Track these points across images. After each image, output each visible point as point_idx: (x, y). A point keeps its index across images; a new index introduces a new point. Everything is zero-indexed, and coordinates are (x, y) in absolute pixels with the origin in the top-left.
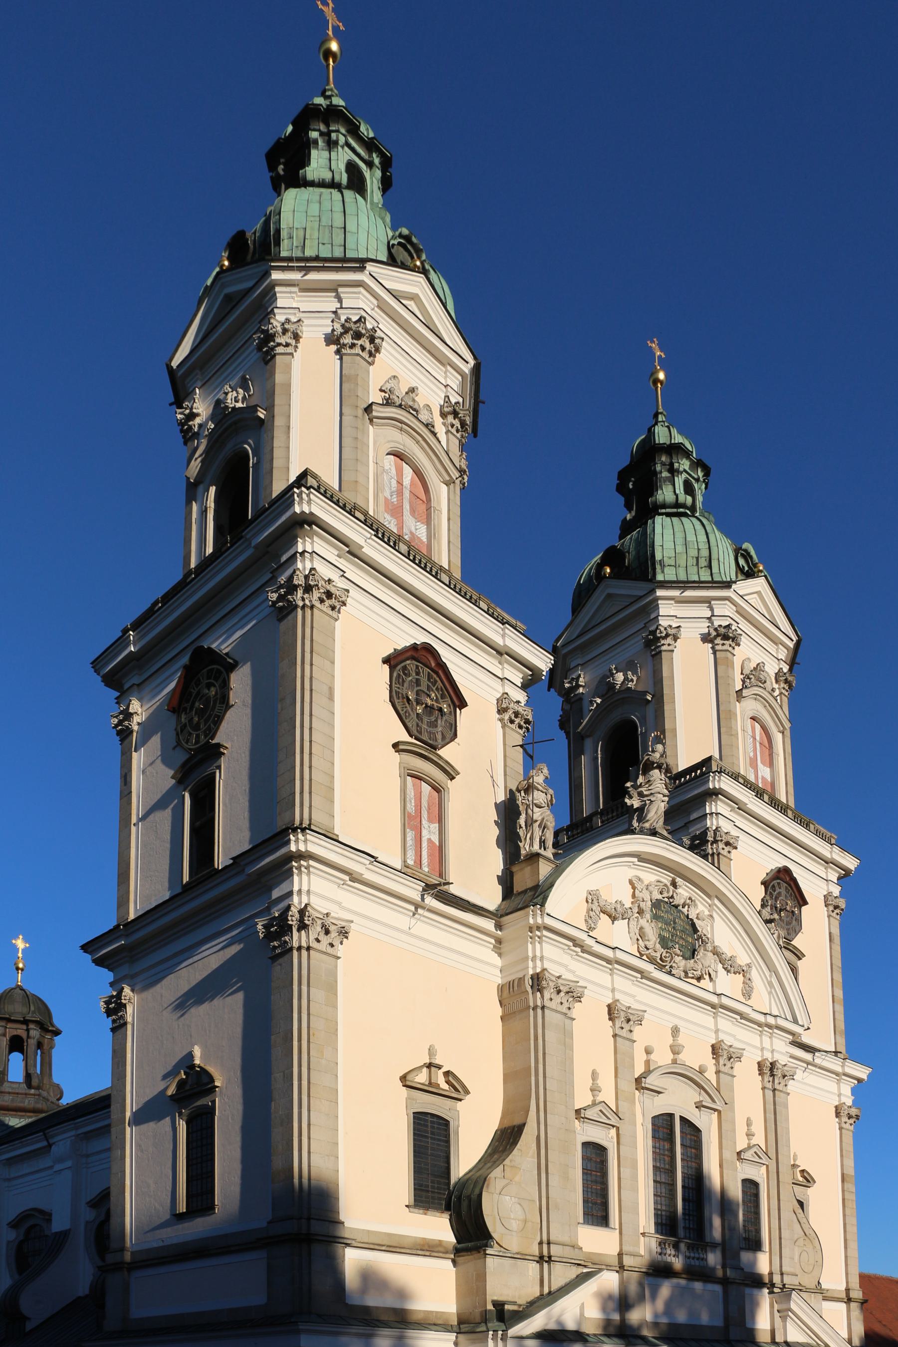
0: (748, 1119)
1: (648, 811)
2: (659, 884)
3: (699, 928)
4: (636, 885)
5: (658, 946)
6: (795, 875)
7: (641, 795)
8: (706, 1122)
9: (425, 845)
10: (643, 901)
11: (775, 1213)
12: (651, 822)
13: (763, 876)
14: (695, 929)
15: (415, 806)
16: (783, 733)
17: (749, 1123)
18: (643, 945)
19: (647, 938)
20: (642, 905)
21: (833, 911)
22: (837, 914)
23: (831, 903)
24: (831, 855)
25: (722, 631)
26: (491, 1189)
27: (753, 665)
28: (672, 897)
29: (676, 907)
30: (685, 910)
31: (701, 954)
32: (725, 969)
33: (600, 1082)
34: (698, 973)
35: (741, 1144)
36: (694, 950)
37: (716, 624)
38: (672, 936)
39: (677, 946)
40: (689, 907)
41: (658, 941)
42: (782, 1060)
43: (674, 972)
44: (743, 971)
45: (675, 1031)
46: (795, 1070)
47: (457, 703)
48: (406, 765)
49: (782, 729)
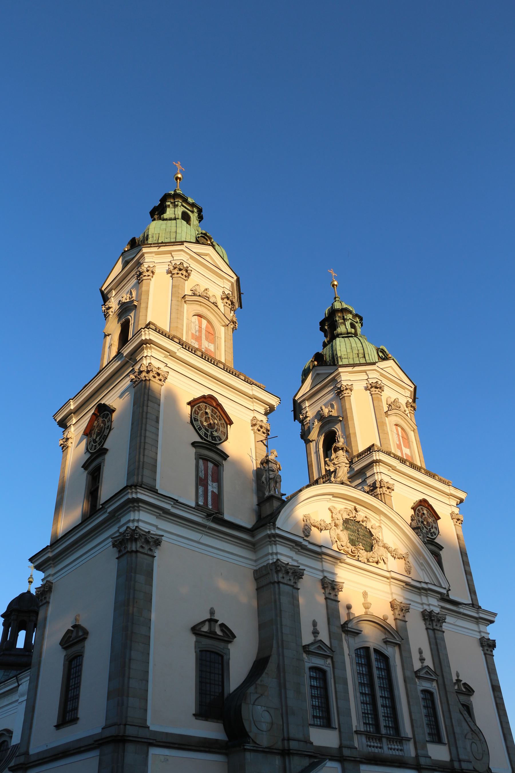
0: (420, 649)
1: (338, 472)
2: (346, 510)
3: (373, 534)
4: (333, 511)
5: (349, 545)
6: (430, 503)
7: (334, 464)
9: (210, 494)
10: (338, 520)
12: (341, 477)
13: (412, 505)
14: (372, 535)
15: (204, 474)
16: (414, 431)
17: (421, 652)
19: (341, 540)
20: (337, 522)
21: (457, 522)
22: (460, 523)
23: (454, 517)
24: (450, 492)
25: (374, 385)
27: (392, 400)
28: (355, 517)
29: (359, 522)
30: (364, 524)
31: (376, 548)
32: (393, 556)
33: (319, 628)
34: (376, 560)
36: (372, 546)
37: (370, 382)
38: (358, 539)
39: (361, 544)
40: (366, 522)
41: (348, 541)
42: (437, 610)
43: (360, 559)
44: (404, 557)
45: (365, 594)
46: (445, 616)
47: (228, 422)
48: (198, 453)
49: (413, 429)
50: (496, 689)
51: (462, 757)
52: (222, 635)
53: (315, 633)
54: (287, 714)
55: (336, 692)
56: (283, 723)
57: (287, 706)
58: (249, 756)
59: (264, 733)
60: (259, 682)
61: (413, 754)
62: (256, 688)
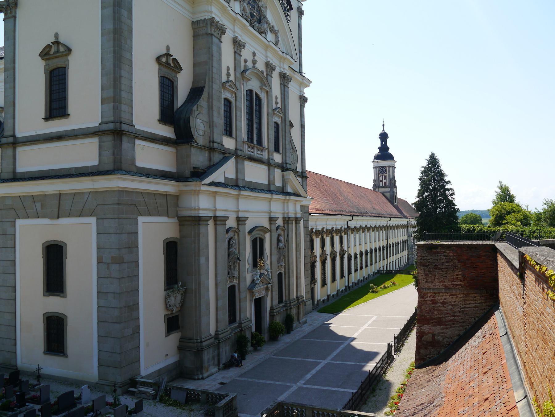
8: (262, 95)
11: (284, 137)
18: (244, 14)
26: (193, 115)
35: (274, 107)
45: (254, 54)
50: (302, 126)
51: (288, 162)
52: (173, 66)
53: (228, 75)
54: (213, 126)
55: (236, 116)
56: (210, 132)
57: (213, 121)
58: (193, 150)
59: (201, 137)
60: (198, 103)
61: (267, 158)
62: (197, 107)
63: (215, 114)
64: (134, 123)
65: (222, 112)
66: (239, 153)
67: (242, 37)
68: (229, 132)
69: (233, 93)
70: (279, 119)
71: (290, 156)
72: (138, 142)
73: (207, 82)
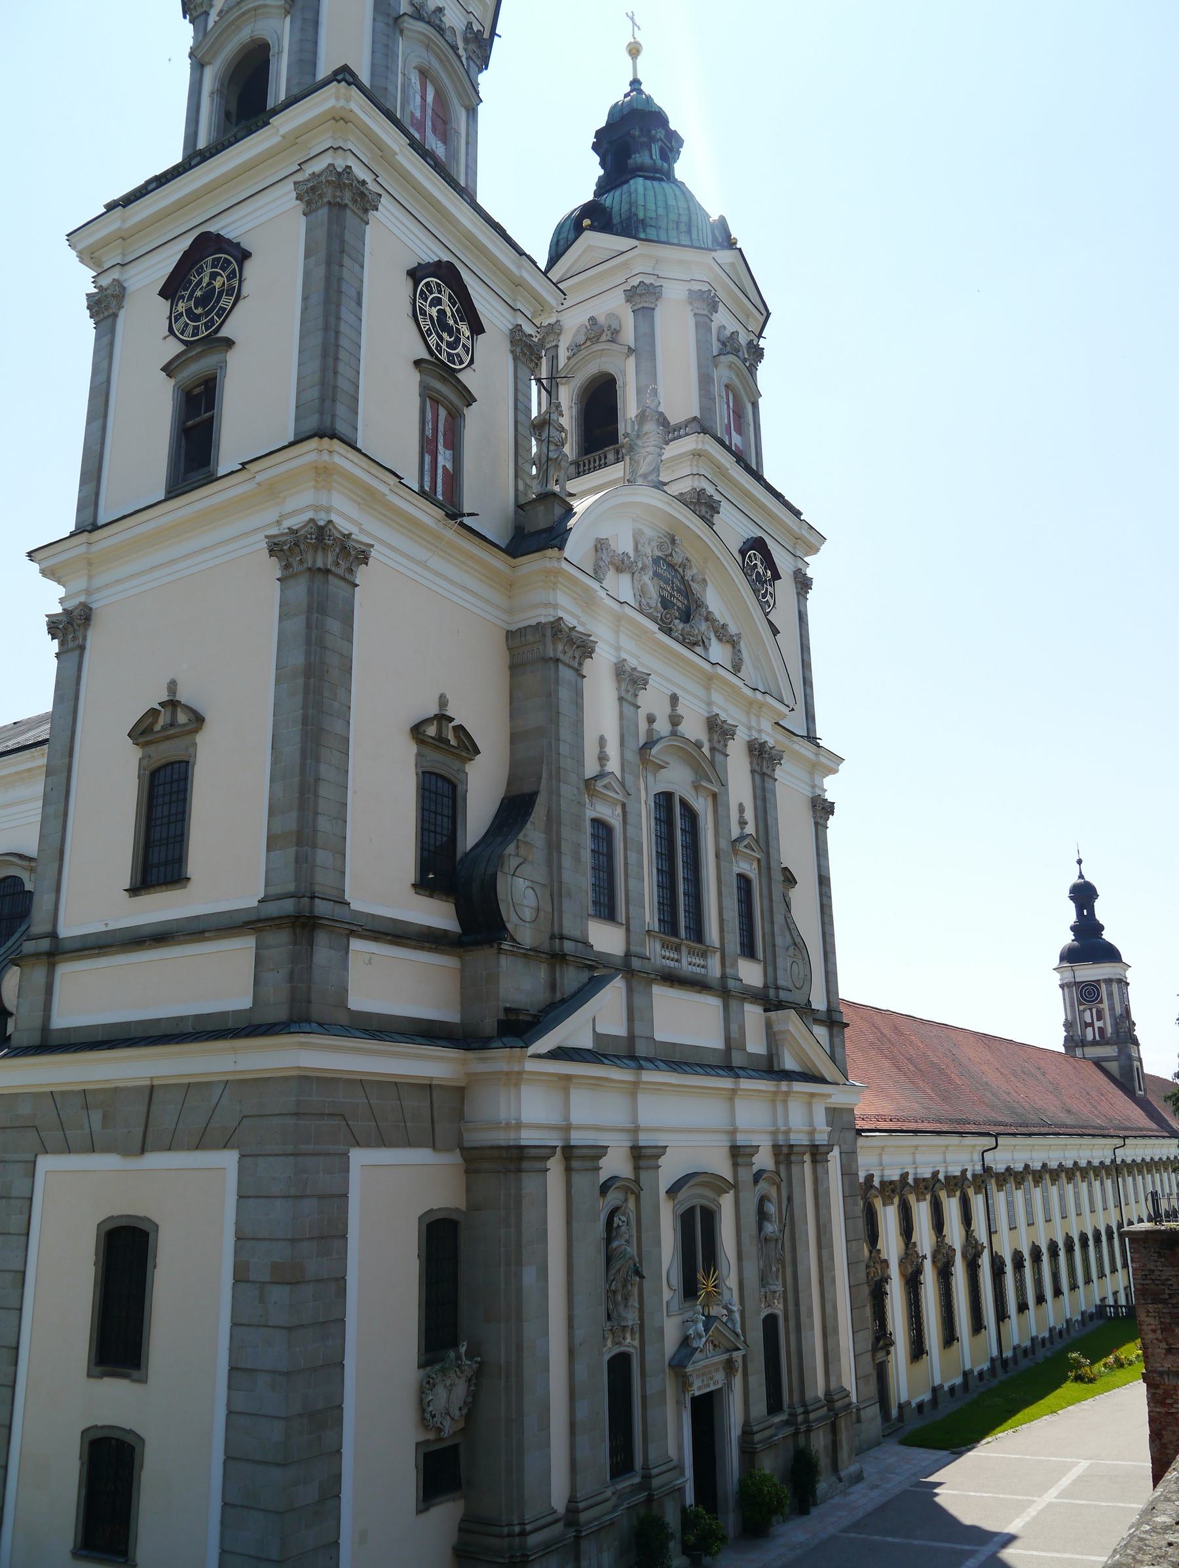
8: (701, 805)
11: (766, 914)
26: (506, 870)
35: (735, 832)
45: (674, 699)
51: (781, 982)
55: (626, 864)
56: (553, 910)
59: (528, 925)
60: (521, 837)
63: (567, 862)
64: (347, 897)
65: (587, 856)
66: (636, 963)
67: (639, 659)
68: (606, 910)
69: (616, 805)
70: (751, 864)
71: (789, 965)
72: (356, 945)
73: (544, 781)
